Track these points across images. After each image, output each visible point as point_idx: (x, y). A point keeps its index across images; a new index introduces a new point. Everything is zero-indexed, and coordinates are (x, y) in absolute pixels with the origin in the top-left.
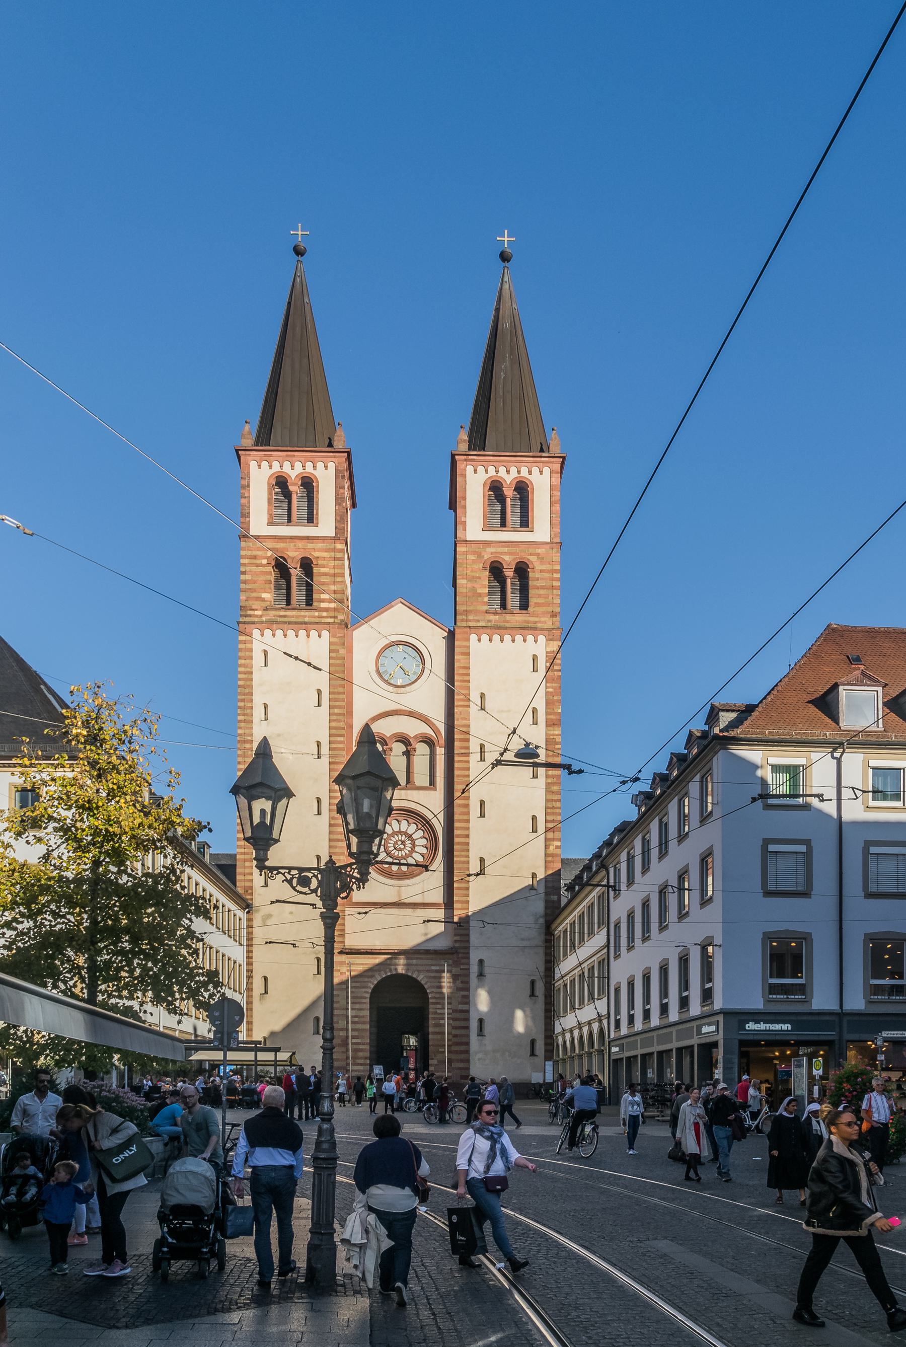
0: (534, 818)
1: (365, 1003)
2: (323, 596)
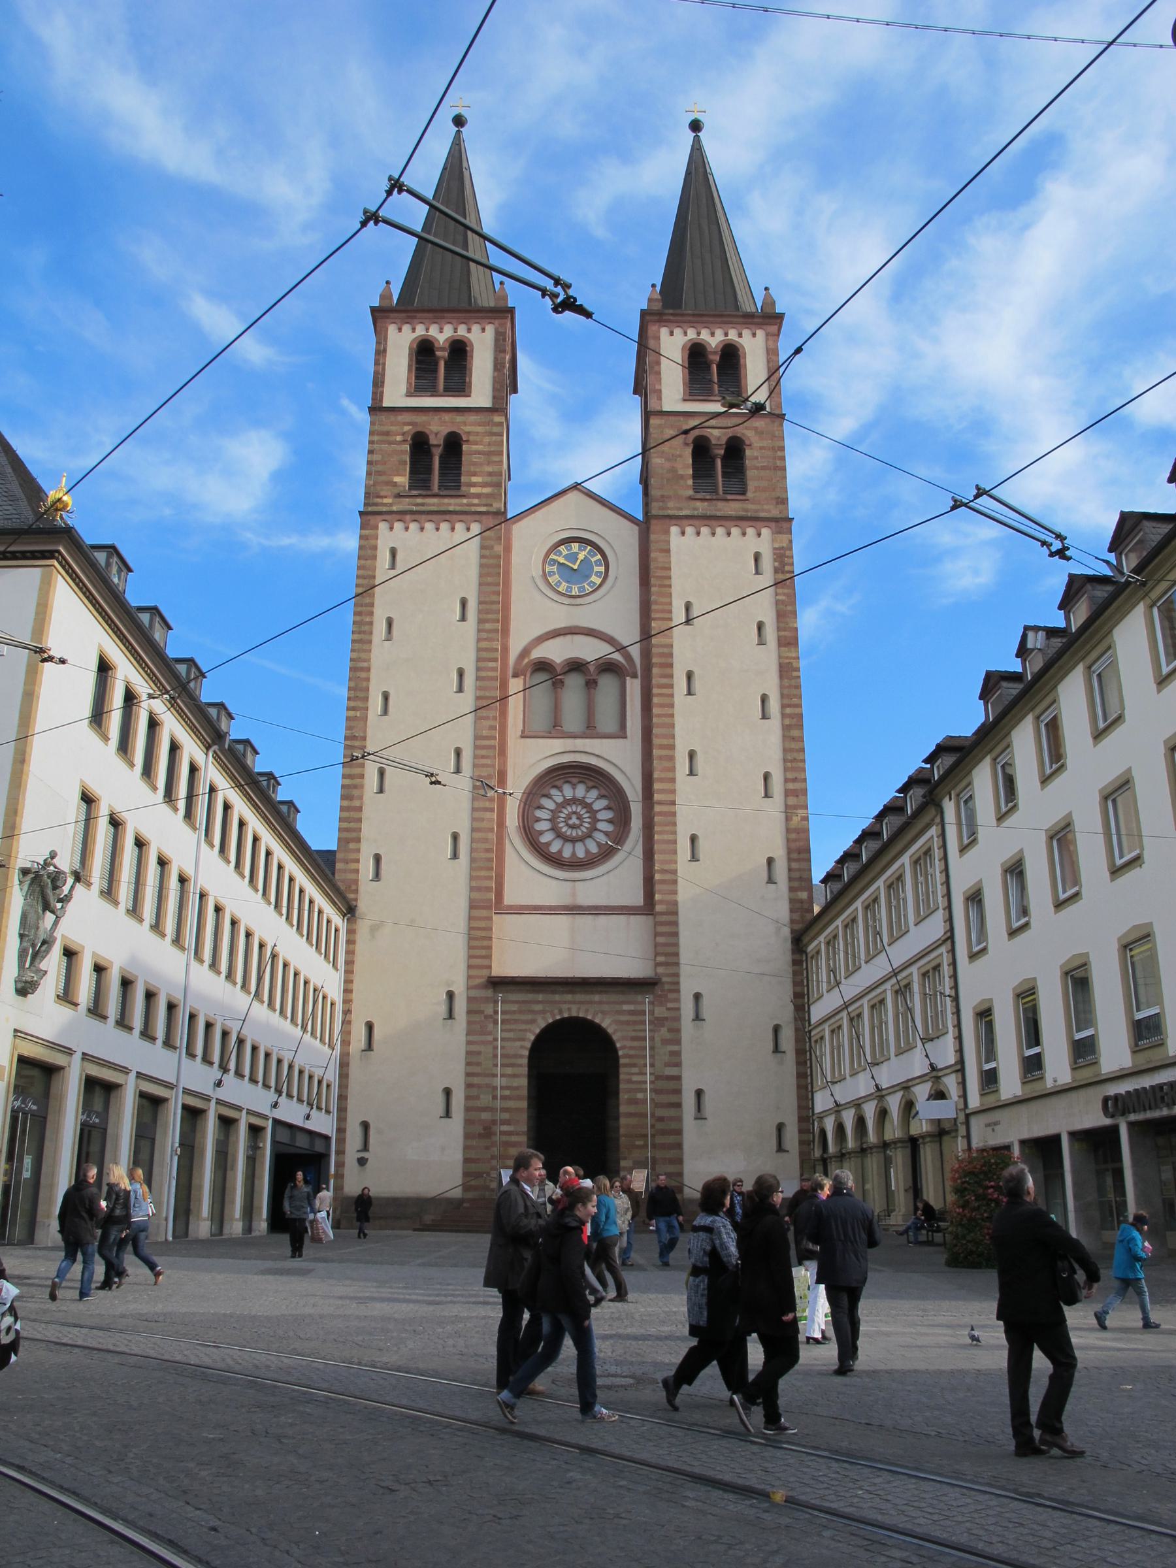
0: (767, 777)
1: (520, 1066)
2: (474, 479)
